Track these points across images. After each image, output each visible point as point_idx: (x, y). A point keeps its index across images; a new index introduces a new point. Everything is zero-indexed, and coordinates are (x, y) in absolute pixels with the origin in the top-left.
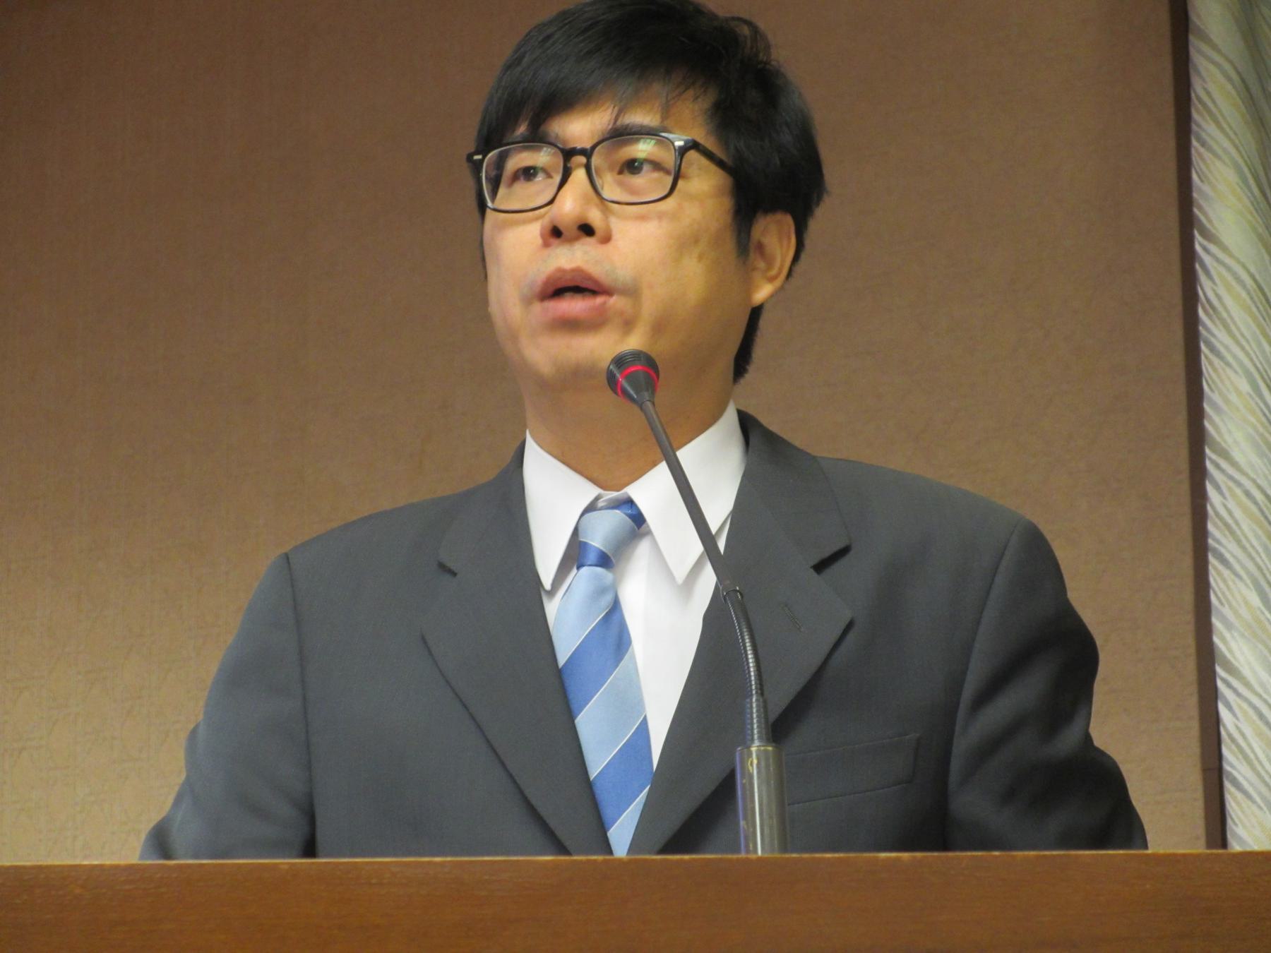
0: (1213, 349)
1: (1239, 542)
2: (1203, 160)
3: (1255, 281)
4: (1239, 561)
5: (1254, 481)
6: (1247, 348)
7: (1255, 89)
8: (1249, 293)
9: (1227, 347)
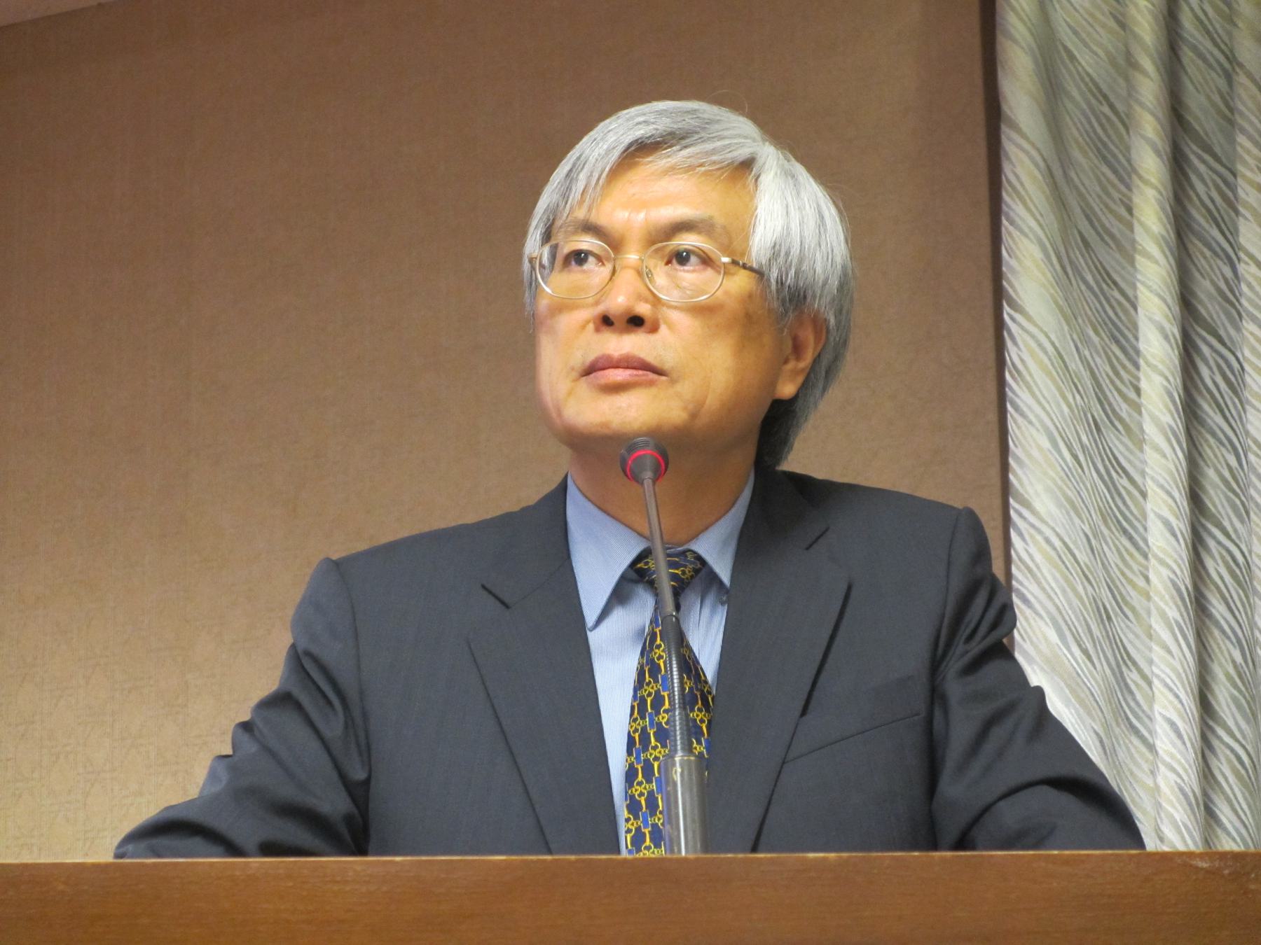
0: (1017, 409)
1: (1039, 584)
4: (1040, 602)
9: (1030, 408)
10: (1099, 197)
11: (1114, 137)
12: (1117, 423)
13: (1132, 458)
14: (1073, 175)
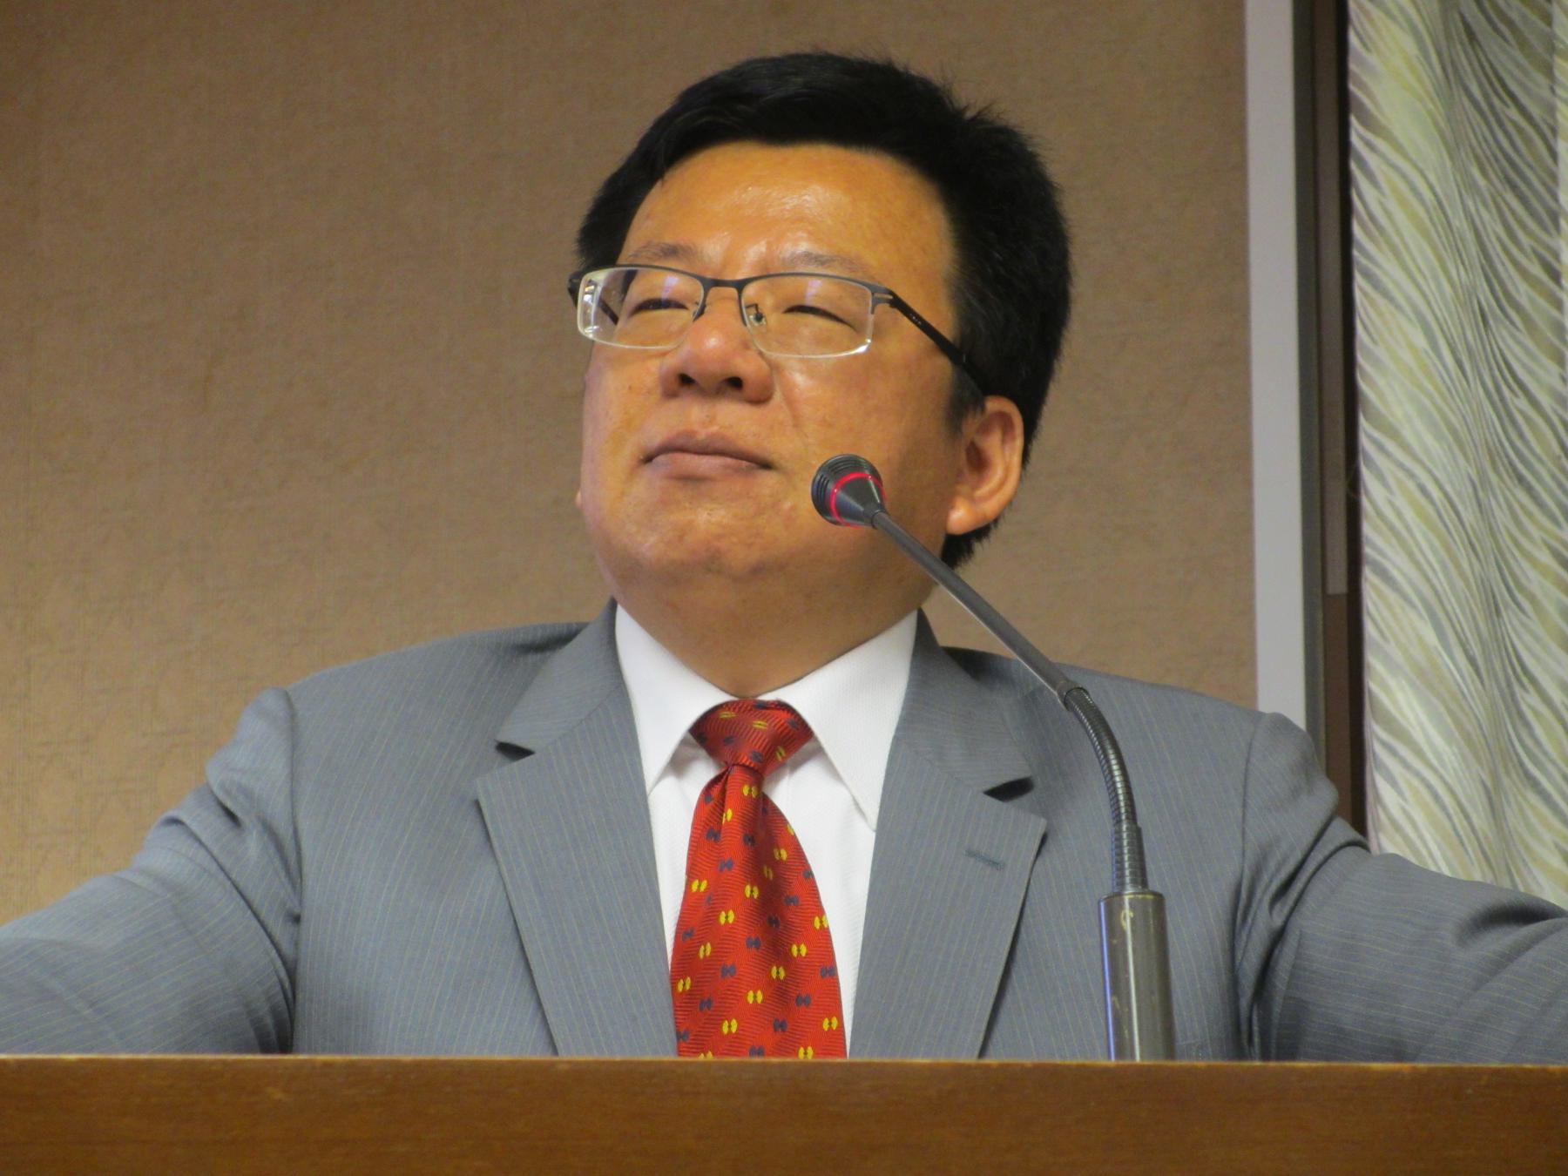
1: (1411, 555)
2: (1371, 20)
3: (1435, 194)
5: (1430, 472)
6: (1425, 288)
8: (1428, 212)
13: (1534, 366)
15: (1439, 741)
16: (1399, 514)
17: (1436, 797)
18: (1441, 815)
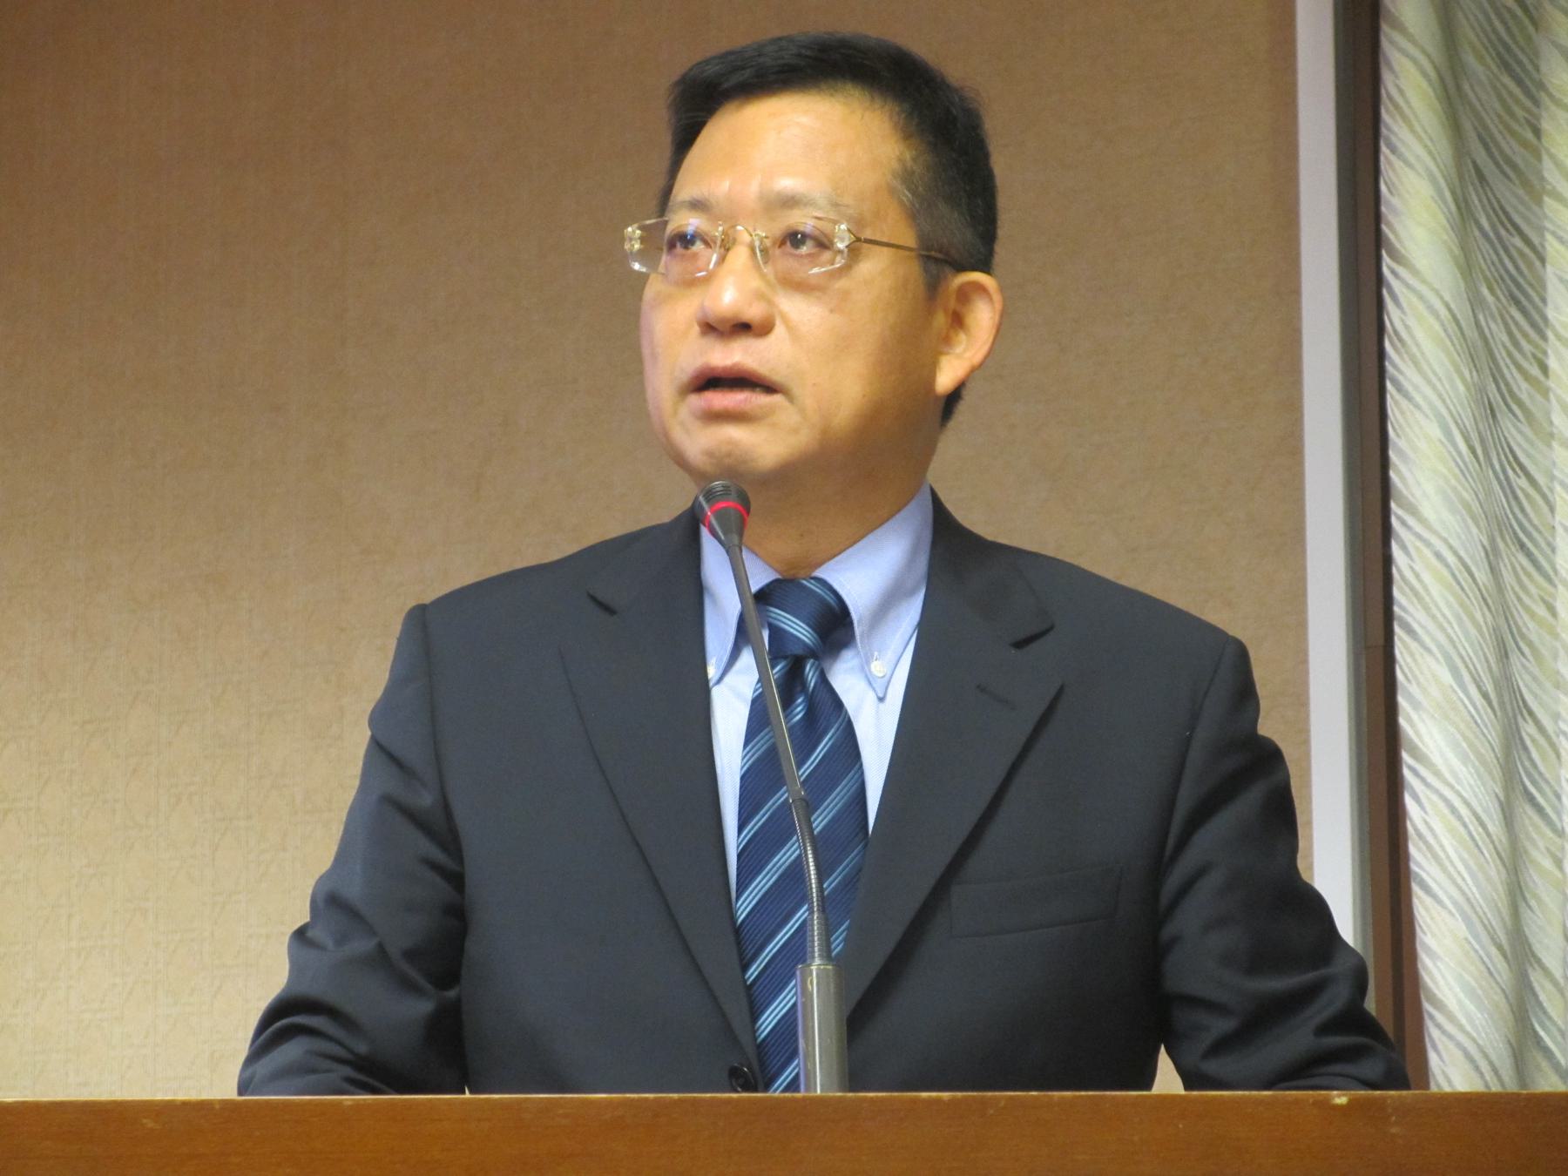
0: (1399, 388)
1: (1427, 609)
2: (1394, 170)
3: (1450, 310)
4: (1428, 632)
5: (1445, 541)
7: (1452, 91)
8: (1443, 325)
9: (1416, 388)
10: (1499, 116)
11: (1519, 38)
12: (1515, 407)
13: (1531, 451)
14: (1466, 87)
15: (1456, 762)
16: (1417, 576)
17: (1454, 810)
18: (1457, 824)
